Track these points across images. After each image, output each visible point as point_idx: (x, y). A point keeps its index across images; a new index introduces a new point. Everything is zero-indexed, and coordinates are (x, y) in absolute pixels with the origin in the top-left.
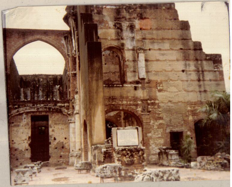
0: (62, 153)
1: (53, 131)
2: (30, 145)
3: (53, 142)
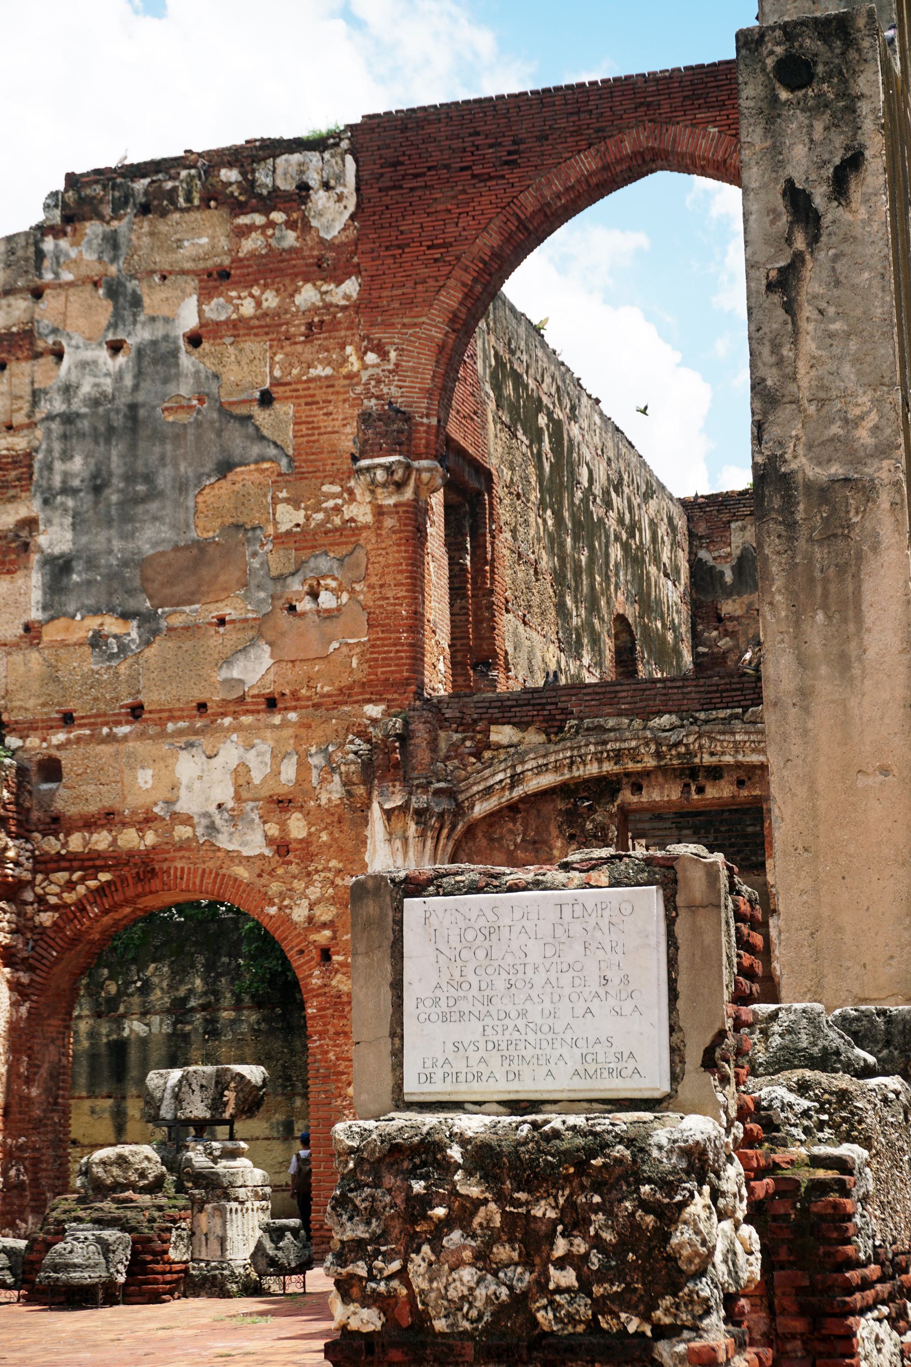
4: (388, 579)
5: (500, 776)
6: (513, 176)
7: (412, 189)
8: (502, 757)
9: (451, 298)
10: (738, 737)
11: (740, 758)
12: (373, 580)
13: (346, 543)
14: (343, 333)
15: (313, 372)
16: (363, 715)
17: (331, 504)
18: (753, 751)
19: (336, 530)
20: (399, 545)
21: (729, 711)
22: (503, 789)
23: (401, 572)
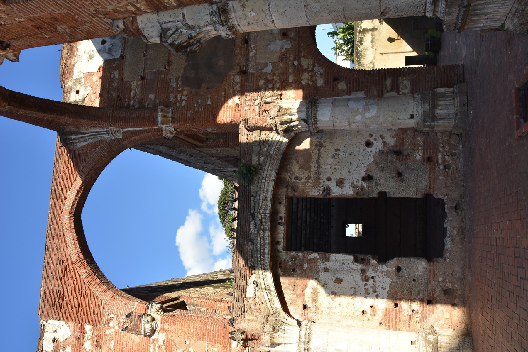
0: (418, 157)
1: (340, 183)
2: (383, 260)
3: (377, 184)
4: (187, 330)
5: (265, 294)
6: (66, 262)
7: (63, 300)
8: (259, 294)
9: (98, 290)
10: (261, 198)
11: (269, 199)
12: (186, 336)
13: (171, 345)
14: (102, 334)
15: (112, 348)
16: (235, 349)
17: (157, 349)
18: (267, 193)
19: (166, 348)
20: (175, 324)
21: (252, 202)
22: (271, 294)
23: (185, 324)
